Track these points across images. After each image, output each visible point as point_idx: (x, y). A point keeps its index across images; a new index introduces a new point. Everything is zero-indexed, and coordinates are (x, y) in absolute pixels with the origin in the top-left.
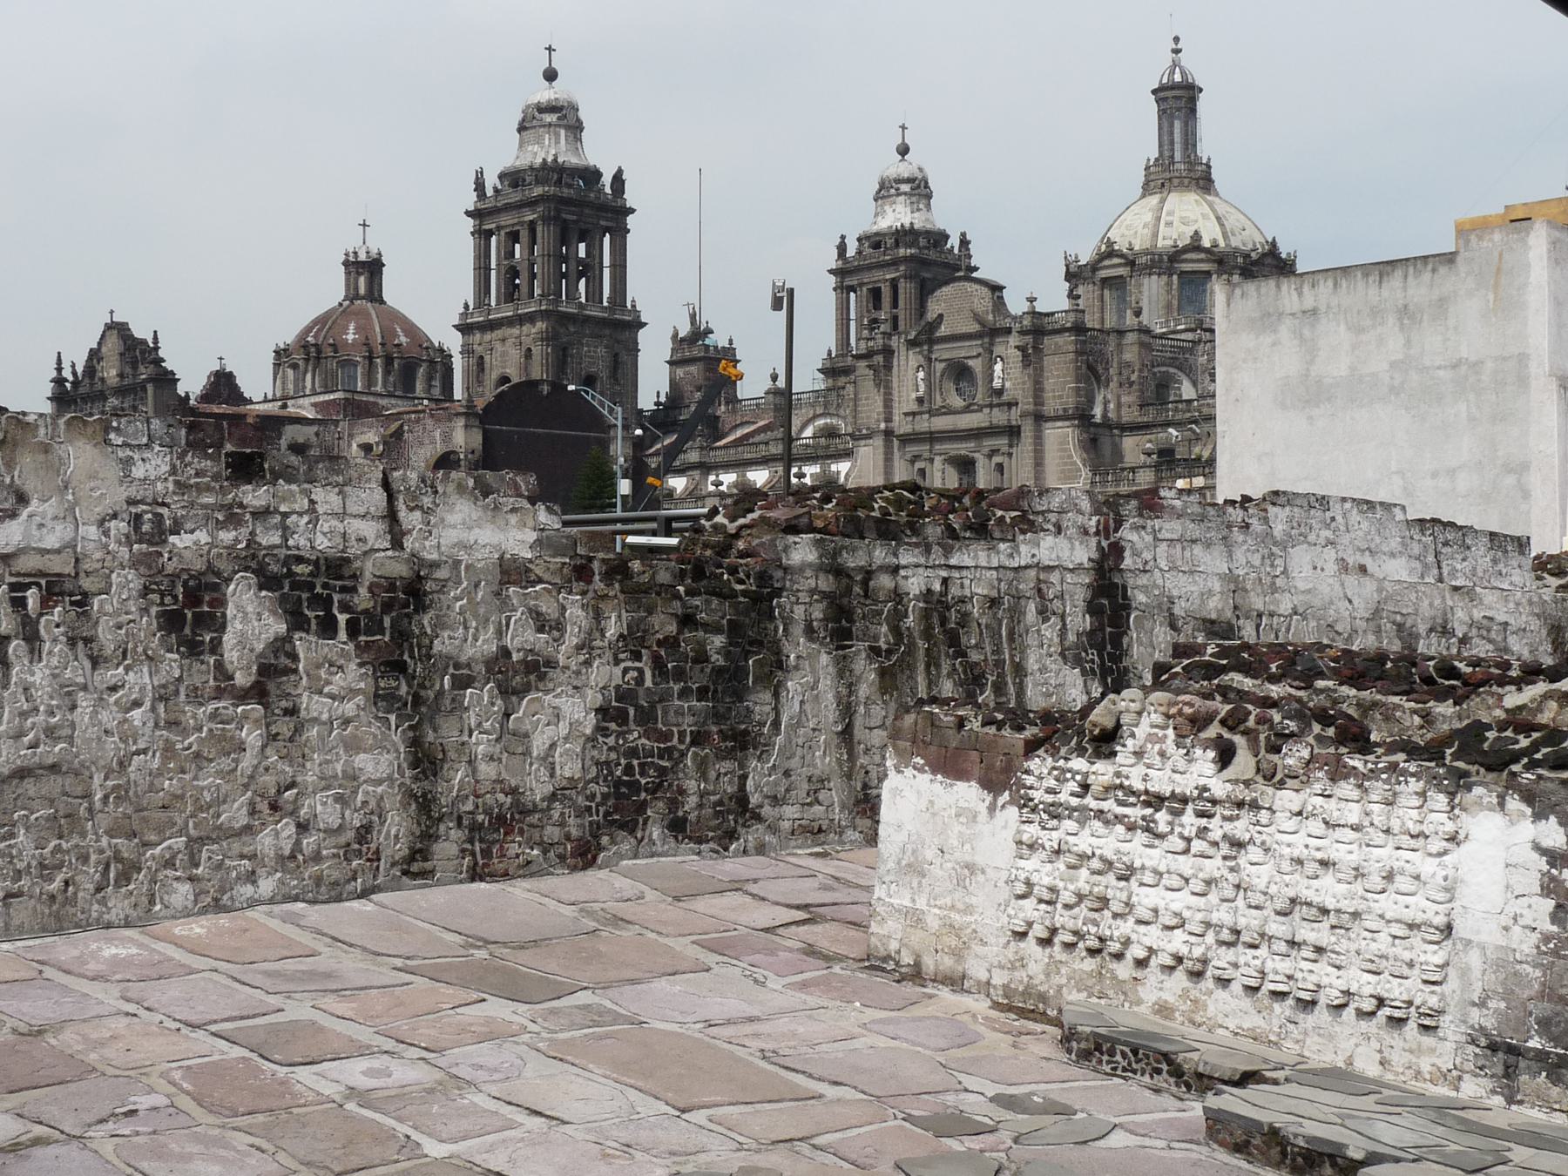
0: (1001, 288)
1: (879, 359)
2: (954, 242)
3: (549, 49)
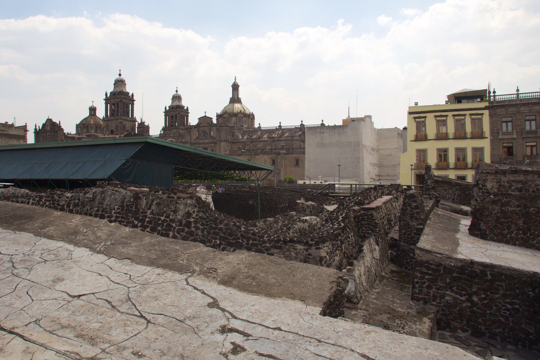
0: (212, 119)
1: (189, 130)
2: (185, 108)
3: (120, 70)
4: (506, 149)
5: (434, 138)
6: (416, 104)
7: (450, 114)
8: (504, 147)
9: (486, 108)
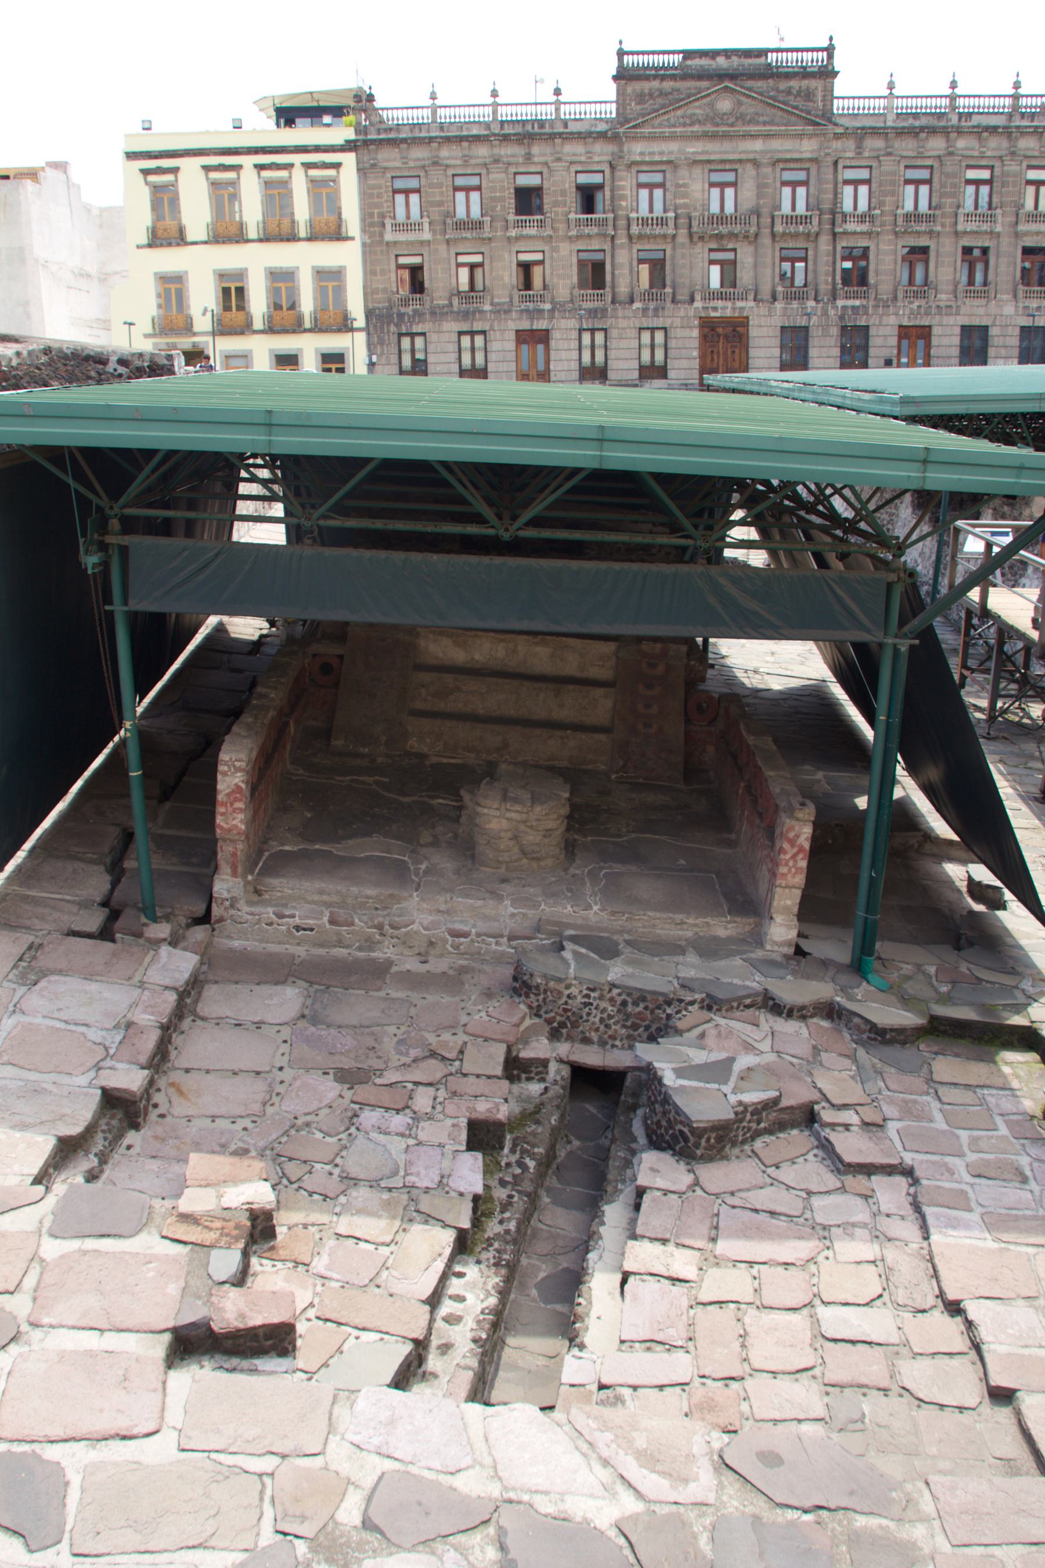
4: (406, 275)
5: (205, 238)
6: (147, 126)
7: (248, 161)
8: (400, 267)
9: (349, 146)
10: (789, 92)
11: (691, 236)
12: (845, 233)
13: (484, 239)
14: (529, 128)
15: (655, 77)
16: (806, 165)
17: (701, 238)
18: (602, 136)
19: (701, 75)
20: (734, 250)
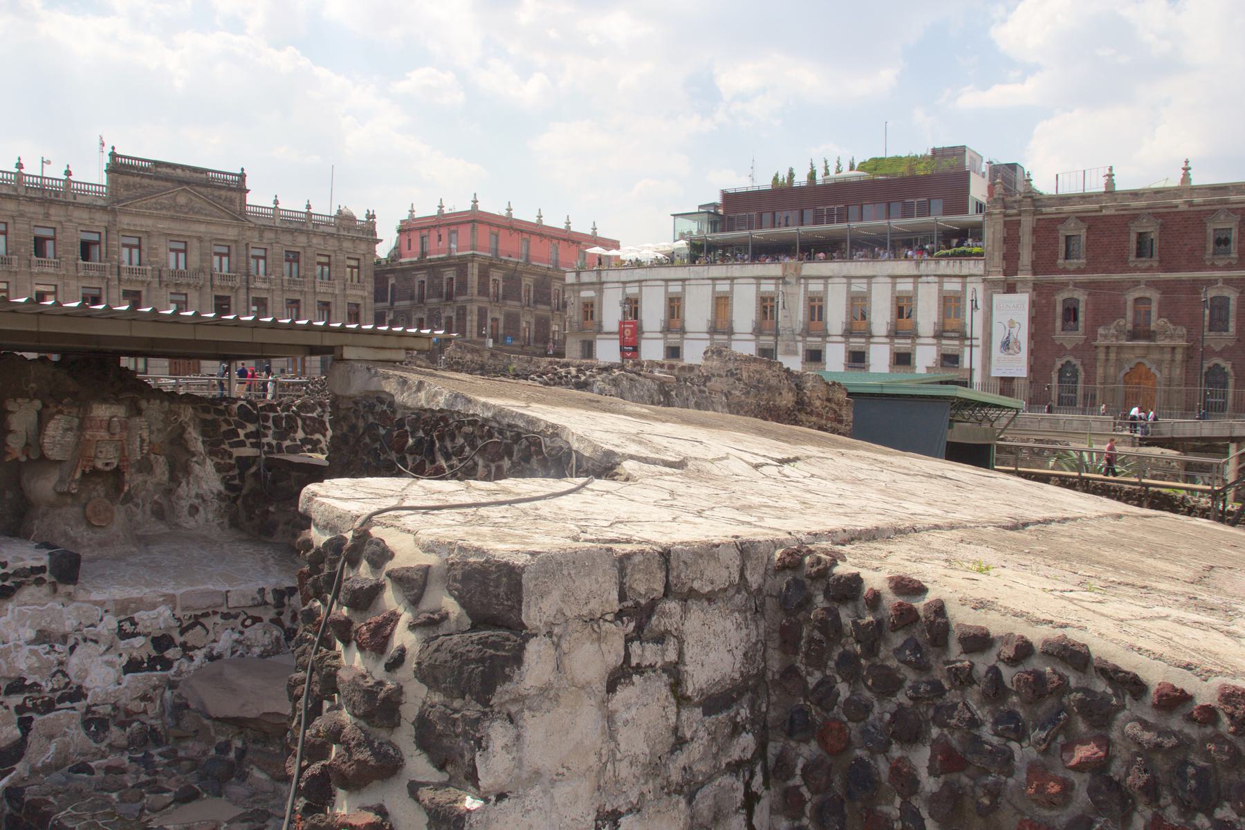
10: (220, 198)
11: (160, 282)
12: (256, 288)
13: (10, 272)
14: (47, 195)
15: (138, 175)
16: (229, 244)
17: (167, 285)
18: (103, 209)
19: (167, 179)
20: (186, 295)
